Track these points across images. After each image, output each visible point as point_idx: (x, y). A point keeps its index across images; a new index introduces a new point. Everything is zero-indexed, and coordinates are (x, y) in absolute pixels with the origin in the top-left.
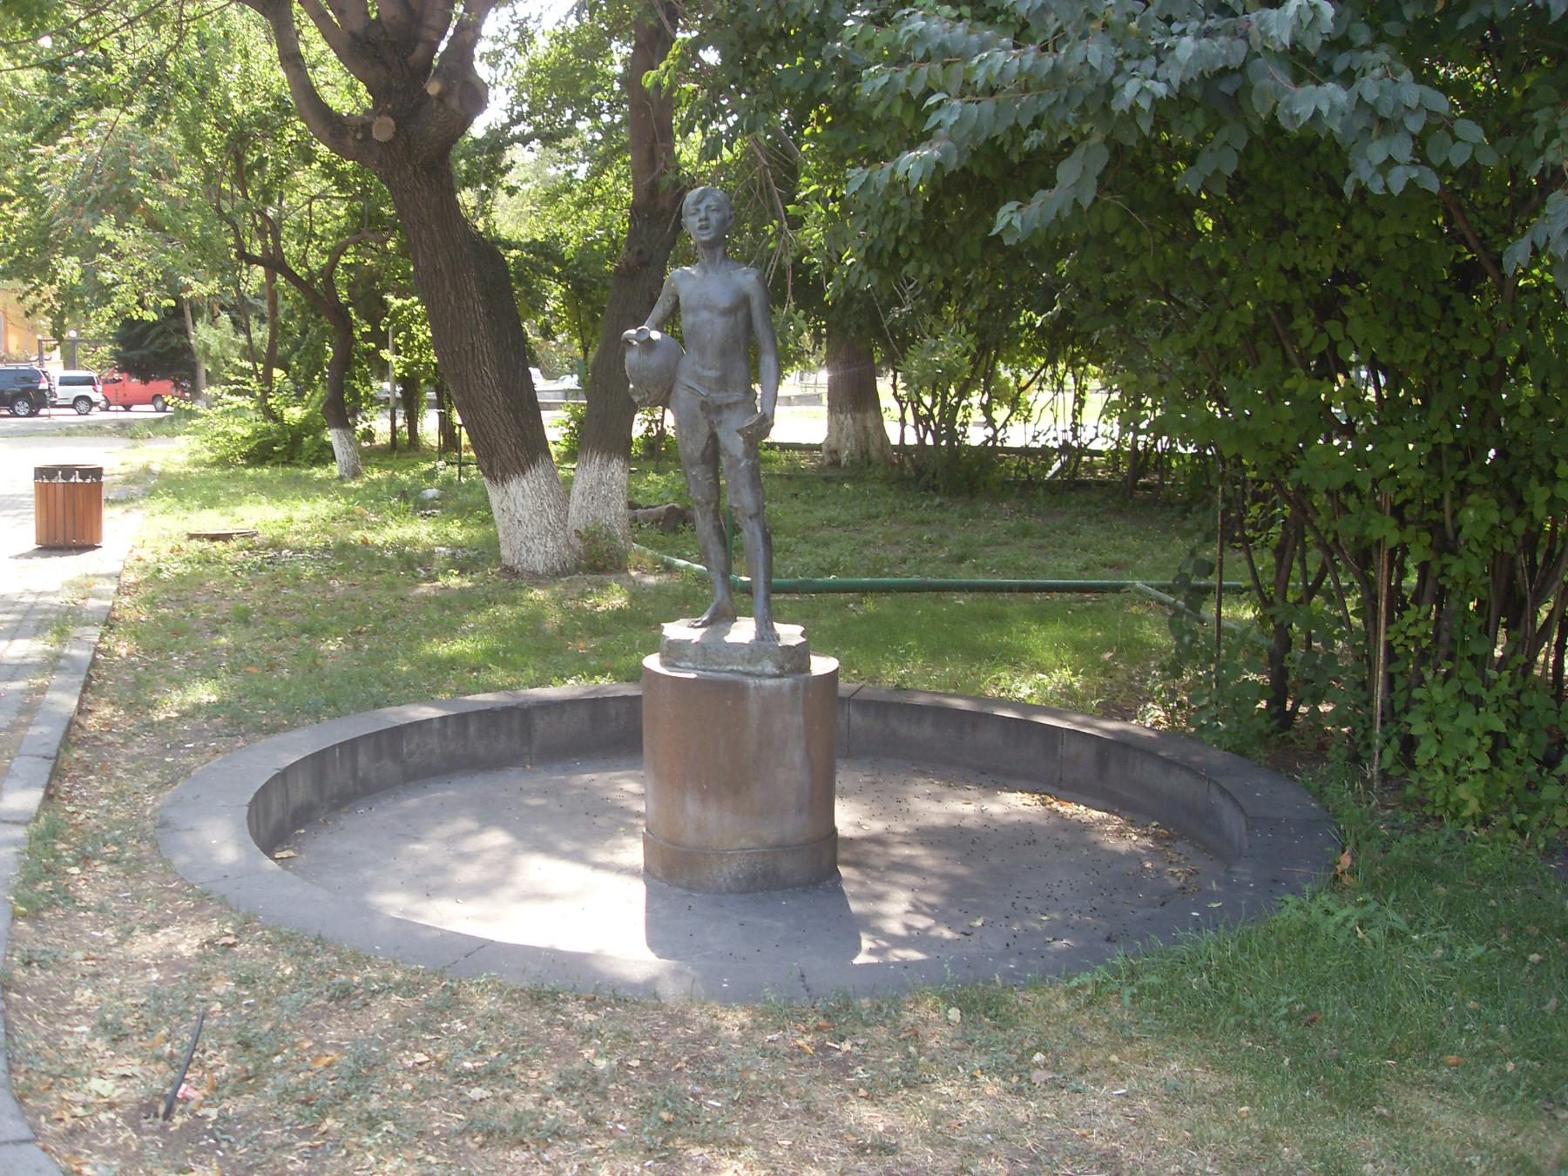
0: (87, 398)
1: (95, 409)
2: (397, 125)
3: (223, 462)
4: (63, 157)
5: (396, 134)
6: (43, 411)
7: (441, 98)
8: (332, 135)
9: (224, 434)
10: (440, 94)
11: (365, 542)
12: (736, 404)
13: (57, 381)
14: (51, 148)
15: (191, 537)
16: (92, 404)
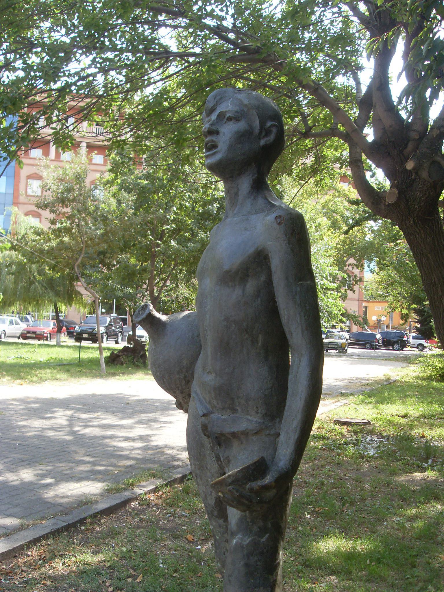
0: (422, 345)
1: (426, 349)
2: (399, 193)
3: (430, 378)
4: (396, 248)
5: (399, 198)
6: (405, 349)
7: (416, 169)
8: (373, 203)
9: (431, 365)
10: (414, 168)
11: (423, 437)
12: (245, 433)
13: (411, 337)
14: (392, 244)
15: (337, 422)
16: (424, 347)
